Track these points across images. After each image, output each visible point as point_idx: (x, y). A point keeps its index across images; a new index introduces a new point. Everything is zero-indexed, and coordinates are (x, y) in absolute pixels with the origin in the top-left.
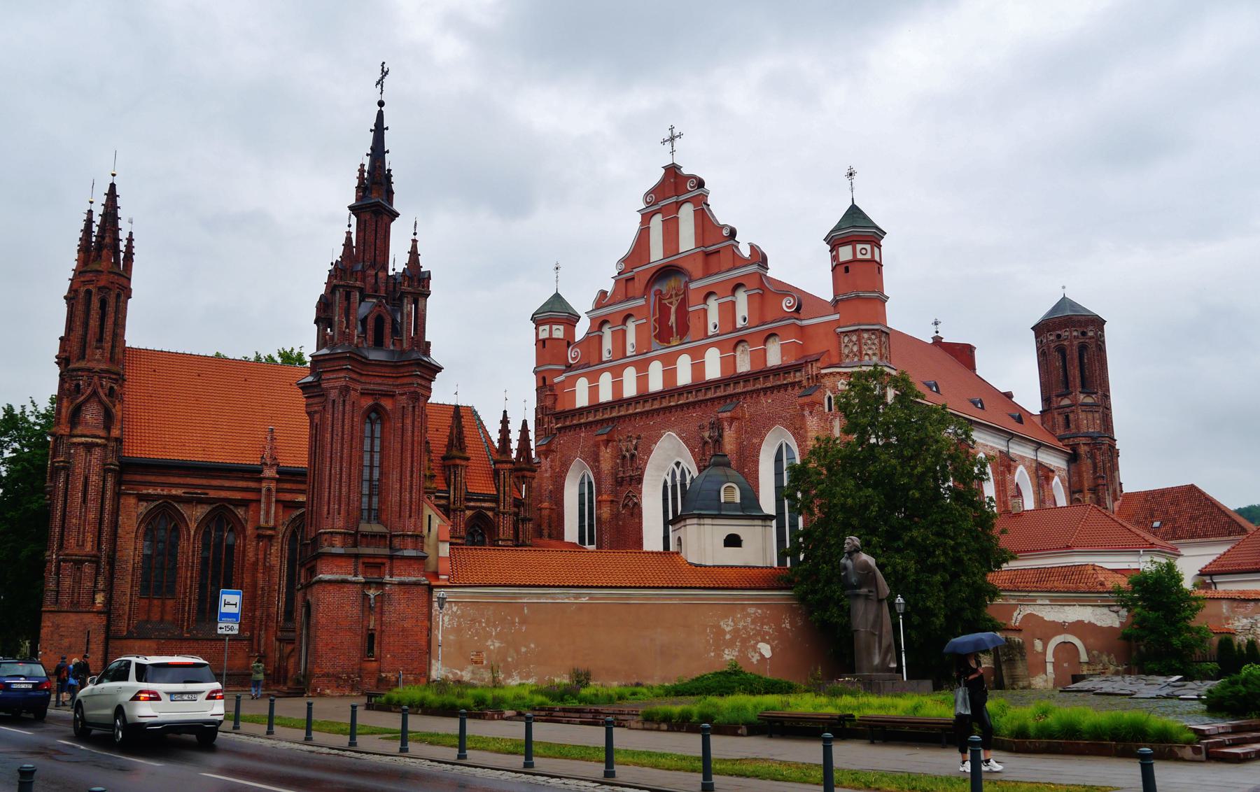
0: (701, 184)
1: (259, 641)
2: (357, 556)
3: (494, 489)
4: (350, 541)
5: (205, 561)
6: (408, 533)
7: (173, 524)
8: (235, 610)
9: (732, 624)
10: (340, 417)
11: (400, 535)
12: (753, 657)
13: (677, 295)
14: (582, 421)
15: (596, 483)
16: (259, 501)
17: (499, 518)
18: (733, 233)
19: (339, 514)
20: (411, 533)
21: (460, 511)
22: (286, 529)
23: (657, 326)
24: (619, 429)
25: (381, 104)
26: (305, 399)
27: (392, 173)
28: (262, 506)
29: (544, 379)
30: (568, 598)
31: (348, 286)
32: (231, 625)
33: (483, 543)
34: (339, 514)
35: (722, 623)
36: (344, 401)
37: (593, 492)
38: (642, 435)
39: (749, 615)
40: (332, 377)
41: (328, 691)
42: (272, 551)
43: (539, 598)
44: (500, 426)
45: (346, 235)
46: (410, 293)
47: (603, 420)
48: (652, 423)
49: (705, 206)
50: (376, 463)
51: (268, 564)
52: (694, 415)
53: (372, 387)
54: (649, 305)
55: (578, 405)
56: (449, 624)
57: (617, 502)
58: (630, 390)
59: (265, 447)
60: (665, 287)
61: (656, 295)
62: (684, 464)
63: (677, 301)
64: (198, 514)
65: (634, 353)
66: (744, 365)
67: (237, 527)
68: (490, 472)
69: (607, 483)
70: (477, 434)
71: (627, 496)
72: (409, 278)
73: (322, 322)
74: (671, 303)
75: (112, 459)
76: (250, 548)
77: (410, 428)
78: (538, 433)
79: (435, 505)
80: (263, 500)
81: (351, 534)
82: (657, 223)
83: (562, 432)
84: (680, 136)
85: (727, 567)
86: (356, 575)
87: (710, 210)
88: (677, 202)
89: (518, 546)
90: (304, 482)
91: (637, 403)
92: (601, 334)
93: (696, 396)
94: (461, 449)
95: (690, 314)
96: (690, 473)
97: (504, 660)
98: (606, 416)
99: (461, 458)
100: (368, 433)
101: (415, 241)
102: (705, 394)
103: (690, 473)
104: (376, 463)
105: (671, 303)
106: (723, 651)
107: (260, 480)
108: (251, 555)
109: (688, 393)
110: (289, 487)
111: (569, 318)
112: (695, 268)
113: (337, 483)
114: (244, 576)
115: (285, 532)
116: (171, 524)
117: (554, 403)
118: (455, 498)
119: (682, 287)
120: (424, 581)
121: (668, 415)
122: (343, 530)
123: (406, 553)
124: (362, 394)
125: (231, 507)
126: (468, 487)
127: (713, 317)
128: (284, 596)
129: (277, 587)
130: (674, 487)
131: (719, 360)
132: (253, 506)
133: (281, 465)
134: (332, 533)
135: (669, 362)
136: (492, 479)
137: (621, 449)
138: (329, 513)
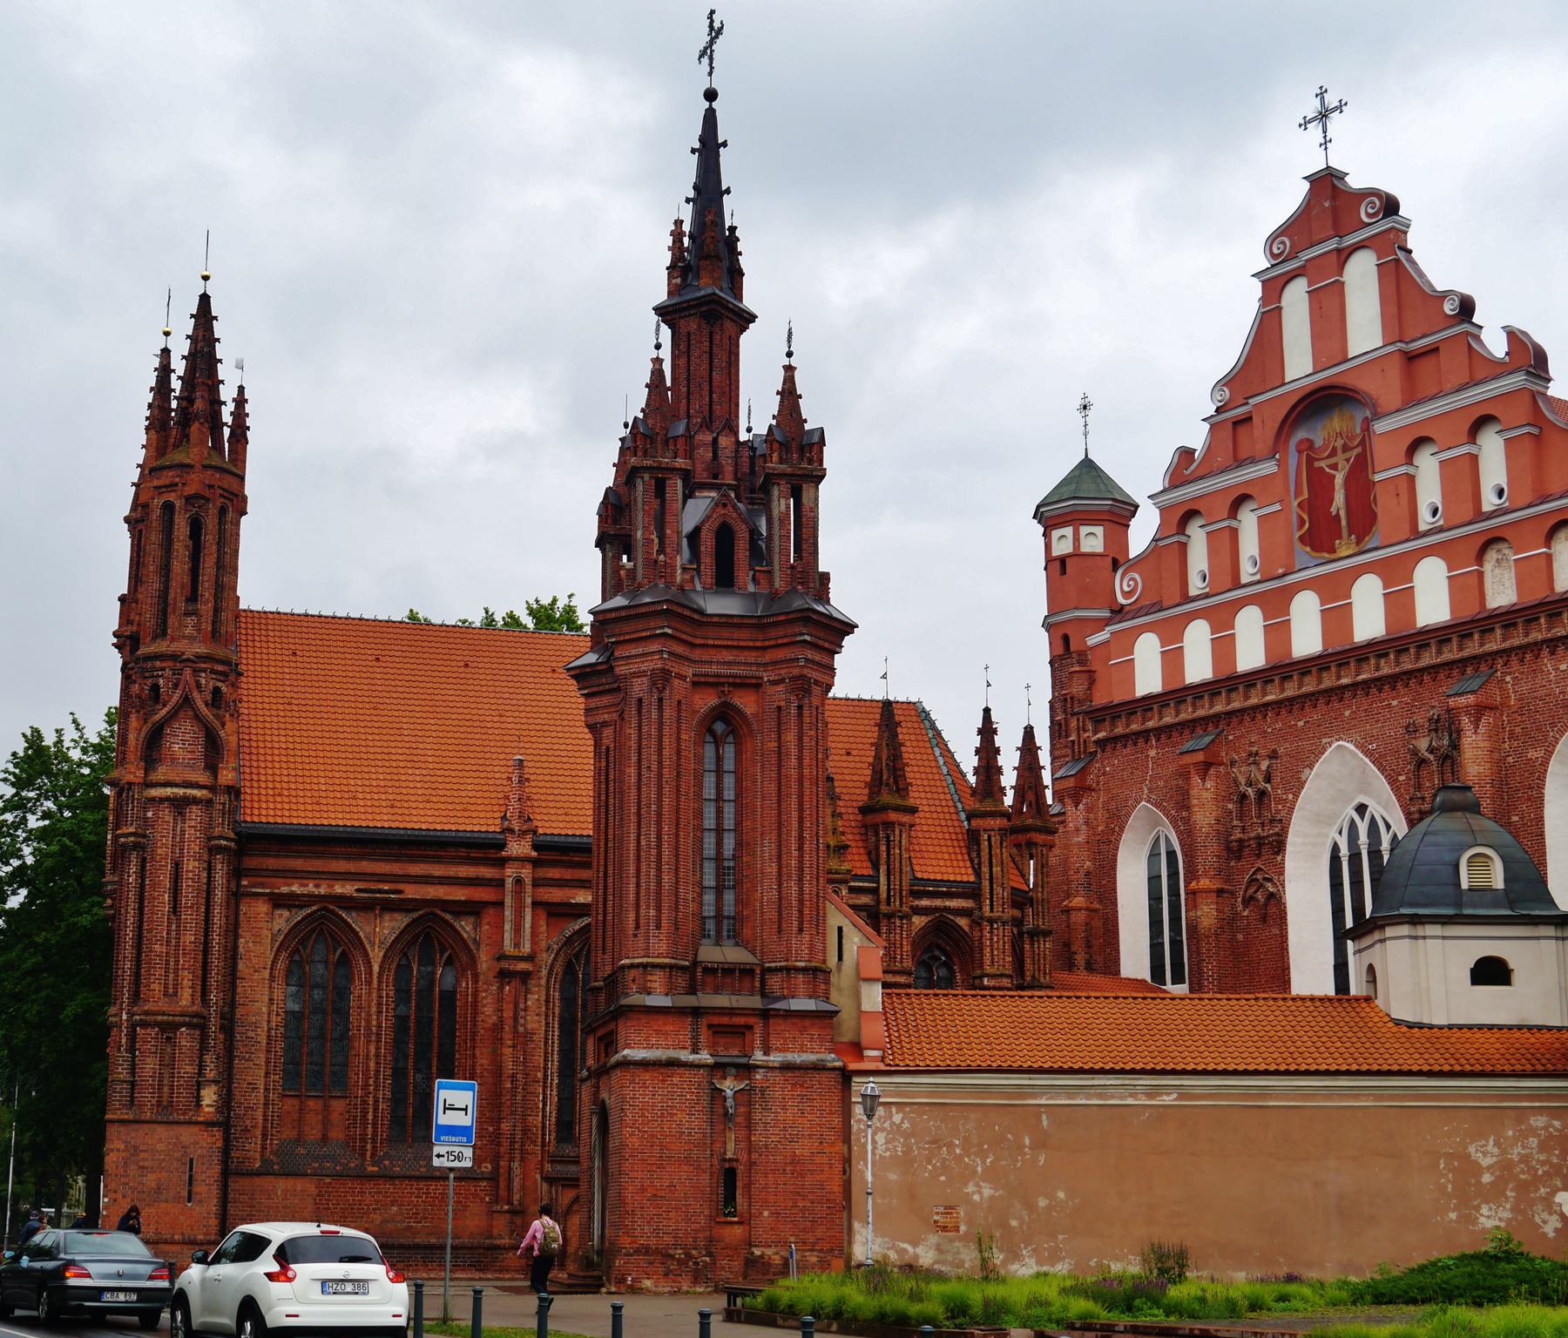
0: (1390, 206)
1: (510, 1180)
2: (696, 1012)
3: (970, 871)
4: (682, 981)
5: (401, 1024)
6: (798, 964)
7: (338, 953)
8: (465, 1120)
9: (1496, 1150)
10: (654, 732)
11: (781, 969)
12: (1545, 1222)
13: (1346, 449)
14: (1150, 724)
15: (1185, 854)
16: (501, 904)
17: (981, 930)
18: (1467, 307)
19: (658, 927)
20: (803, 964)
21: (901, 918)
22: (554, 959)
23: (1306, 517)
24: (1231, 738)
25: (711, 95)
26: (582, 700)
27: (738, 233)
28: (507, 913)
29: (1066, 639)
30: (1132, 1095)
31: (659, 469)
32: (457, 1149)
33: (949, 983)
34: (658, 927)
35: (1472, 1149)
36: (660, 700)
37: (1177, 873)
38: (1281, 751)
39: (1533, 1131)
40: (634, 652)
41: (648, 1283)
42: (529, 1003)
43: (1070, 1097)
44: (976, 741)
45: (651, 365)
46: (783, 475)
47: (1193, 721)
48: (1301, 724)
49: (1401, 255)
50: (729, 822)
51: (521, 1029)
52: (1395, 703)
53: (714, 669)
54: (1286, 473)
55: (1140, 691)
56: (887, 1149)
57: (1232, 893)
58: (1251, 655)
59: (507, 798)
60: (1321, 432)
61: (1300, 452)
62: (1374, 808)
64: (386, 932)
65: (1258, 577)
66: (1501, 592)
67: (461, 956)
68: (960, 837)
69: (1209, 854)
70: (931, 757)
71: (1252, 881)
72: (780, 444)
73: (611, 543)
74: (1334, 467)
75: (222, 829)
76: (486, 998)
77: (794, 751)
78: (1057, 753)
79: (850, 906)
80: (508, 901)
81: (683, 968)
82: (1296, 297)
83: (1108, 748)
84: (1340, 108)
85: (1480, 1027)
86: (695, 1051)
87: (1413, 263)
88: (1338, 251)
89: (1022, 988)
90: (587, 865)
91: (1266, 682)
92: (1183, 539)
93: (1397, 663)
94: (898, 790)
95: (1378, 489)
96: (1388, 827)
97: (1004, 1225)
98: (1201, 713)
99: (897, 809)
100: (710, 763)
101: (789, 369)
102: (1418, 658)
103: (1388, 827)
104: (729, 822)
105: (1334, 467)
106: (1478, 1208)
107: (502, 862)
108: (488, 1010)
109: (1380, 656)
110: (557, 876)
111: (1116, 510)
112: (1384, 388)
113: (653, 865)
114: (477, 1052)
115: (552, 964)
116: (335, 951)
117: (1090, 688)
118: (889, 890)
119: (1358, 431)
120: (834, 1060)
121: (1336, 705)
122: (667, 961)
123: (798, 1004)
124: (694, 684)
125: (448, 917)
126: (916, 868)
127: (1429, 491)
128: (555, 1093)
129: (540, 1075)
130: (1355, 858)
131: (1159, 656)
132: (489, 915)
133: (541, 831)
134: (645, 966)
135: (1335, 591)
136: (964, 850)
137: (1236, 781)
138: (637, 927)
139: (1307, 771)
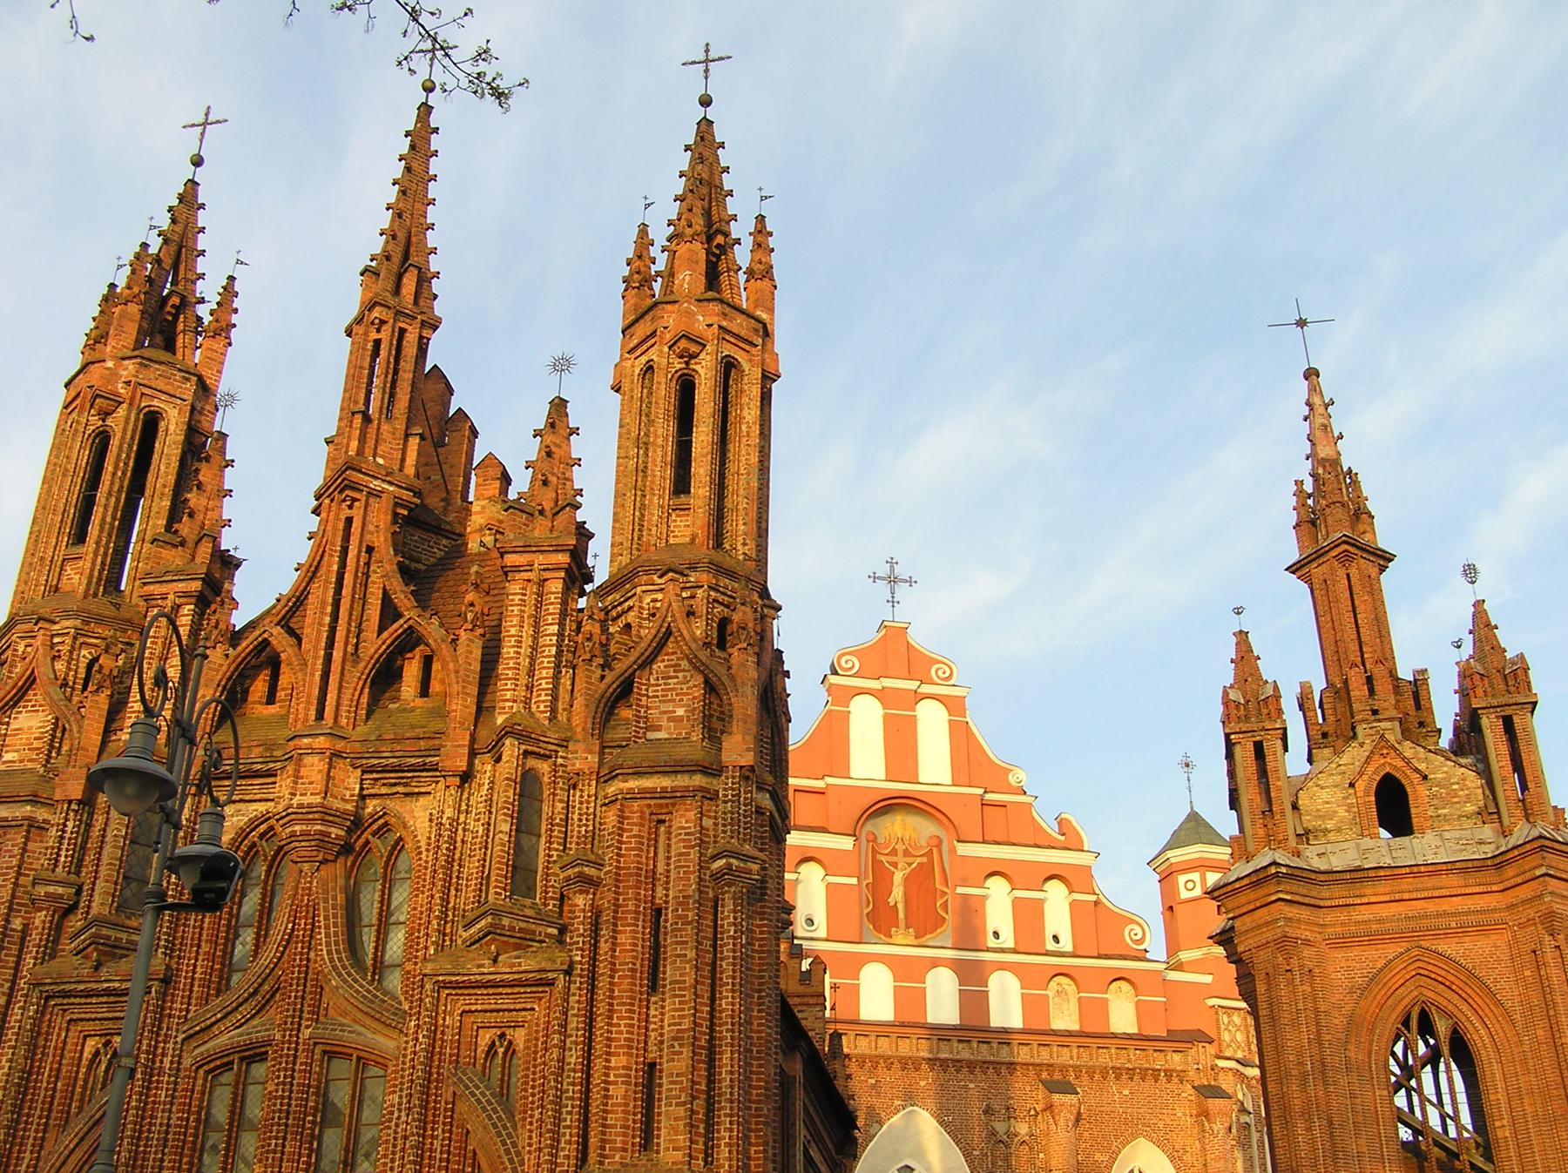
52: (971, 1086)
60: (896, 827)
61: (868, 841)
63: (910, 864)
66: (1064, 1018)
74: (895, 865)
119: (923, 843)
139: (876, 1126)
